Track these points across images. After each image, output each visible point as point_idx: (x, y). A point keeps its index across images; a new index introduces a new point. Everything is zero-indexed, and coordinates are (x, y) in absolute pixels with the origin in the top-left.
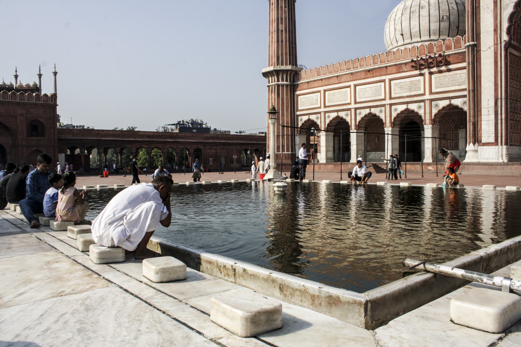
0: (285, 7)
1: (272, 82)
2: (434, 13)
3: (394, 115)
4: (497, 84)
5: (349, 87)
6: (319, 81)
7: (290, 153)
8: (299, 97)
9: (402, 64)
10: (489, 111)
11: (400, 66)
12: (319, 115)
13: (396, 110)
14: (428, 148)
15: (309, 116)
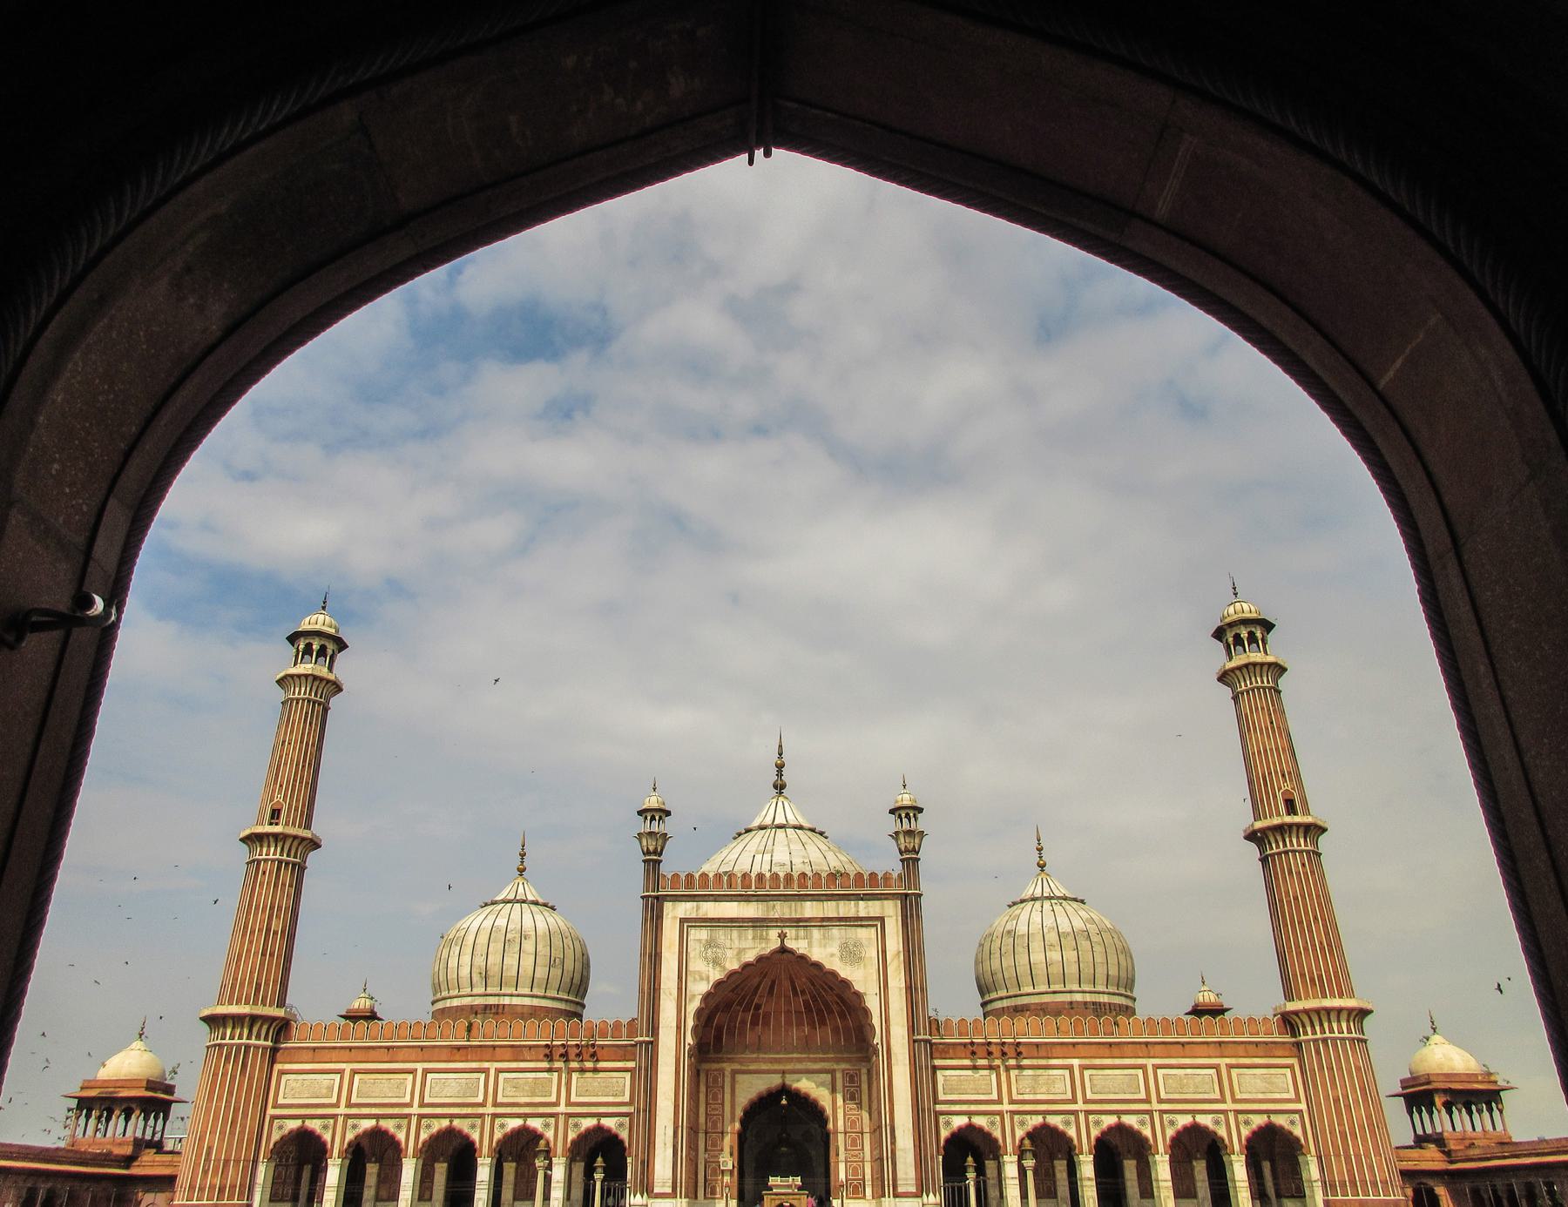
0: (290, 886)
1: (232, 1038)
2: (543, 950)
3: (498, 1135)
4: (679, 1106)
5: (413, 1072)
6: (343, 1051)
7: (245, 1202)
8: (284, 1078)
9: (525, 1046)
10: (665, 1144)
11: (519, 1049)
12: (332, 1121)
13: (502, 1126)
14: (557, 1199)
15: (303, 1122)
